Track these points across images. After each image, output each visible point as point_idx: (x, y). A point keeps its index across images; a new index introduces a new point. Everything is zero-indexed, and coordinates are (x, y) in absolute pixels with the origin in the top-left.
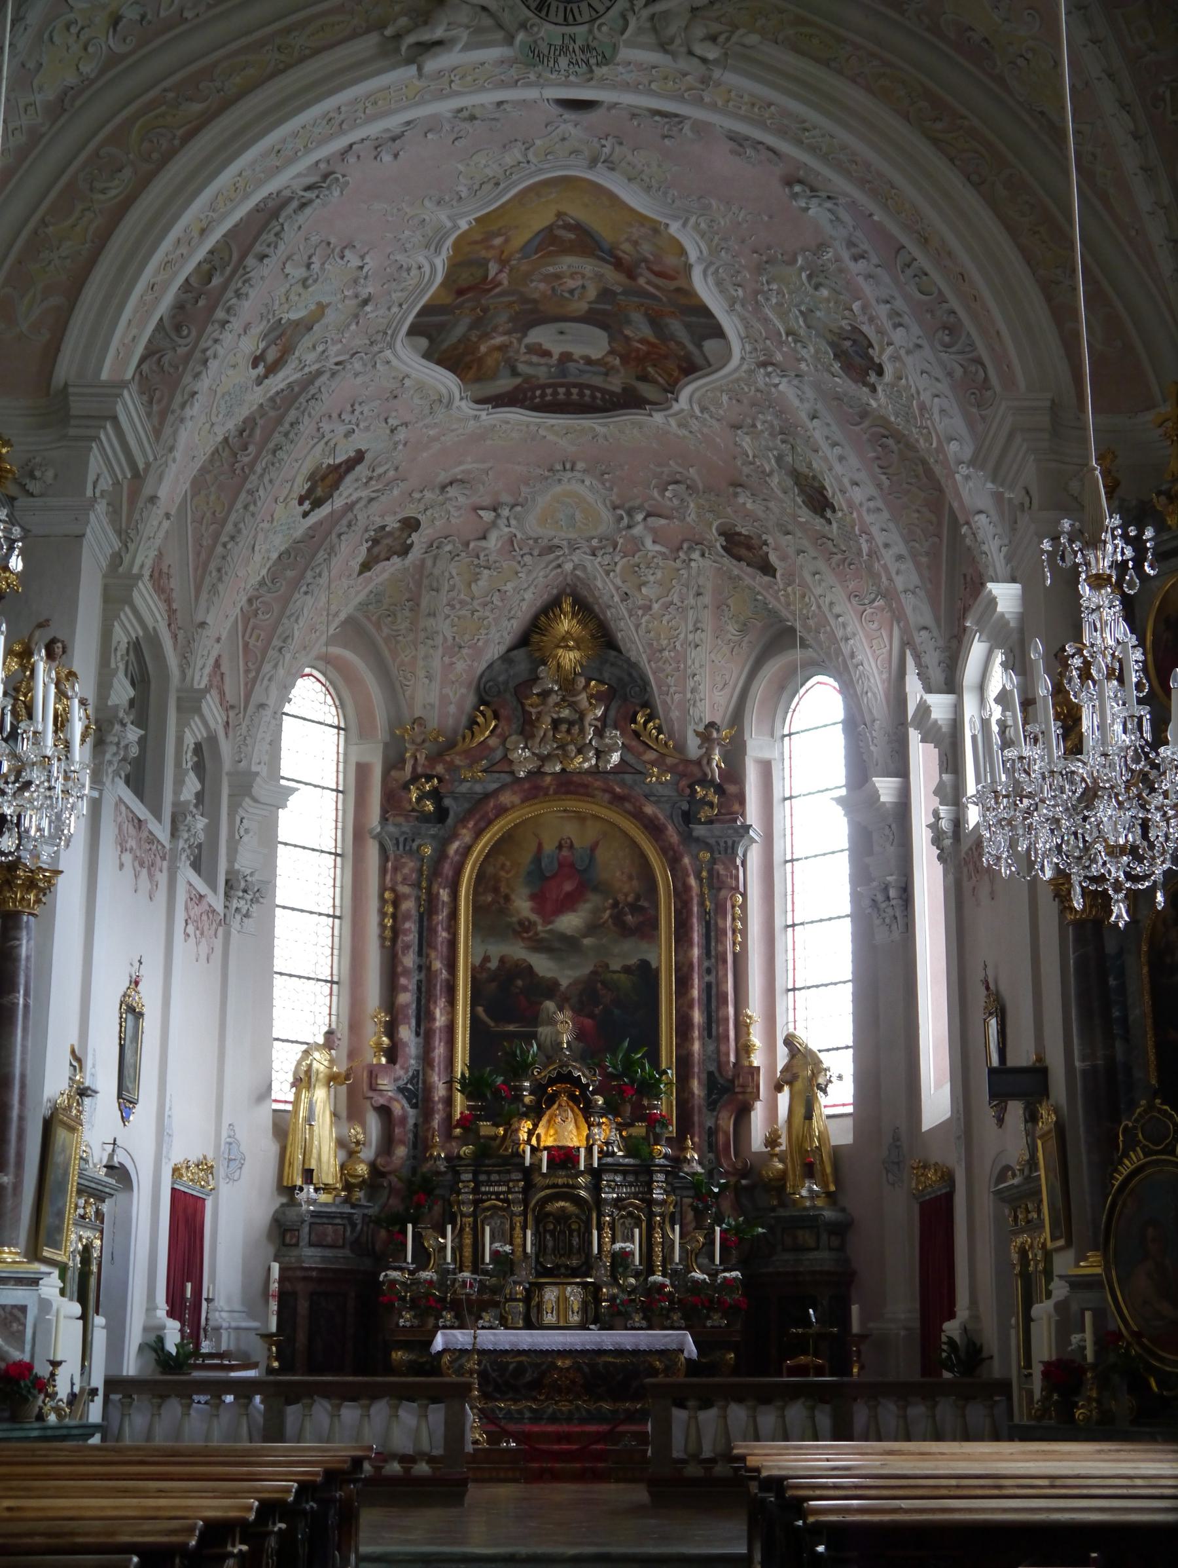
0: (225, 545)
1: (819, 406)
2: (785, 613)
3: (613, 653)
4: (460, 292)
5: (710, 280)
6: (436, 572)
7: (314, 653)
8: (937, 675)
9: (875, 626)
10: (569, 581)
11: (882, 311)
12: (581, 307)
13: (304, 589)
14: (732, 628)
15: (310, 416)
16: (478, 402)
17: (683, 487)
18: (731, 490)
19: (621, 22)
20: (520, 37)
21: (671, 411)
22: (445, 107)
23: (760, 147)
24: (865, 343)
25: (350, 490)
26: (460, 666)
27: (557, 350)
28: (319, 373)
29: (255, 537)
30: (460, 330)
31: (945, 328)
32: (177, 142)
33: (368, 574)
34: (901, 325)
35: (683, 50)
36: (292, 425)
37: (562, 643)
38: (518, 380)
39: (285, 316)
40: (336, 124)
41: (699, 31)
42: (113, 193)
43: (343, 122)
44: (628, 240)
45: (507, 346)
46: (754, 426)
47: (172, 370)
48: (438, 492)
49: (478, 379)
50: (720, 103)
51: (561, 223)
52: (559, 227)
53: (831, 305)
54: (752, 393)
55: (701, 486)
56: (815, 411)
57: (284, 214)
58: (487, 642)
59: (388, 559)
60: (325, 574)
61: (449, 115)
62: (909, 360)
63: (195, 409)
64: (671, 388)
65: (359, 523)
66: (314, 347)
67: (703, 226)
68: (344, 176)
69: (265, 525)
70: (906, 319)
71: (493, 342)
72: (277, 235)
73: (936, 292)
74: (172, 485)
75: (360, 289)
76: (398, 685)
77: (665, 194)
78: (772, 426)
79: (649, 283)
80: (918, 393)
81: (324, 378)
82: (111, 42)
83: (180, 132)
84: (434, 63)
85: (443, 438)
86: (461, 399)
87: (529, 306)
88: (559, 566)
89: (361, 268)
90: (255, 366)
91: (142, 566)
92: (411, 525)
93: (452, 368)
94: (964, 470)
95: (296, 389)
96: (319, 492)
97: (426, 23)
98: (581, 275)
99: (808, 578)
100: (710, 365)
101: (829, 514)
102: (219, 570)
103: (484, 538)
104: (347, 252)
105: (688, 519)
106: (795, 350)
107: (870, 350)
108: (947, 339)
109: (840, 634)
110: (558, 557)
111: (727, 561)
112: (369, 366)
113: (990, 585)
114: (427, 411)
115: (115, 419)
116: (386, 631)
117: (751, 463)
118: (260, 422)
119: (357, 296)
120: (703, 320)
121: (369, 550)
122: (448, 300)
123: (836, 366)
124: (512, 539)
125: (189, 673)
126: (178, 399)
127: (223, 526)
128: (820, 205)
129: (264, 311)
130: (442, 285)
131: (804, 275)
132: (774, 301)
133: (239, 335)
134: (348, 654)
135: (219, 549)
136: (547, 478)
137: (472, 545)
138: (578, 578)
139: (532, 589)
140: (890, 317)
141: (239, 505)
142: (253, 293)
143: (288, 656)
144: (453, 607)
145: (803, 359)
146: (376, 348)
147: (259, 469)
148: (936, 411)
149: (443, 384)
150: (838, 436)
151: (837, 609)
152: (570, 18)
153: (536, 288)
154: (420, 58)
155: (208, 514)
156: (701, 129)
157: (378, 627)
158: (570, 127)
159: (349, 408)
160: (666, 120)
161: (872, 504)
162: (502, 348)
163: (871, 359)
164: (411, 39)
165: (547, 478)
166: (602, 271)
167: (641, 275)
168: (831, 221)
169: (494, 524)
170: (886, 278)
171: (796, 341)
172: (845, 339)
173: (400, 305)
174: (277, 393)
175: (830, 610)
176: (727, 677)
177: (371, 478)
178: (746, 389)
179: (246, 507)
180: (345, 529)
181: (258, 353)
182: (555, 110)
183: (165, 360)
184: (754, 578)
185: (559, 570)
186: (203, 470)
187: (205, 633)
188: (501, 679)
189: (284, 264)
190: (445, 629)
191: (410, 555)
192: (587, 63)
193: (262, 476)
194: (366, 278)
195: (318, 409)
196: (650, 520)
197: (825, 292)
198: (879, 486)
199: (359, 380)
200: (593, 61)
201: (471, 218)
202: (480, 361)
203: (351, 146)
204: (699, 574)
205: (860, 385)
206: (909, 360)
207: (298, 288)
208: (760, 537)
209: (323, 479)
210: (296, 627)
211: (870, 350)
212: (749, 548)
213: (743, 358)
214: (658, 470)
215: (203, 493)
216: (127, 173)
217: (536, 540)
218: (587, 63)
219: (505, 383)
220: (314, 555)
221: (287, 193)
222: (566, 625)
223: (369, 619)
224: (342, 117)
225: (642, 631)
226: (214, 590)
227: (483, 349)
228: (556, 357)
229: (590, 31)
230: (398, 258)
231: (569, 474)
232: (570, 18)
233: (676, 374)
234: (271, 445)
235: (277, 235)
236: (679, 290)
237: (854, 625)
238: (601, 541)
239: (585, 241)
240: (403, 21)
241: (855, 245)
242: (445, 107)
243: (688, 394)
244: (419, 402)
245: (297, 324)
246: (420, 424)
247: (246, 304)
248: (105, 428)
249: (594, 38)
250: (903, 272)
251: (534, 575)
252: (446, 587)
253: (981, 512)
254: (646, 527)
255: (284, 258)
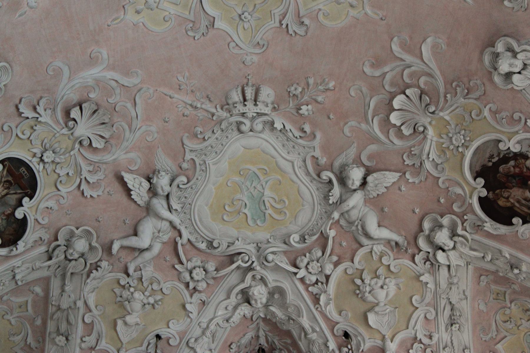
6: (64, 306)
103: (136, 234)
105: (428, 165)
191: (21, 244)
214: (377, 73)
231: (251, 109)
254: (367, 201)
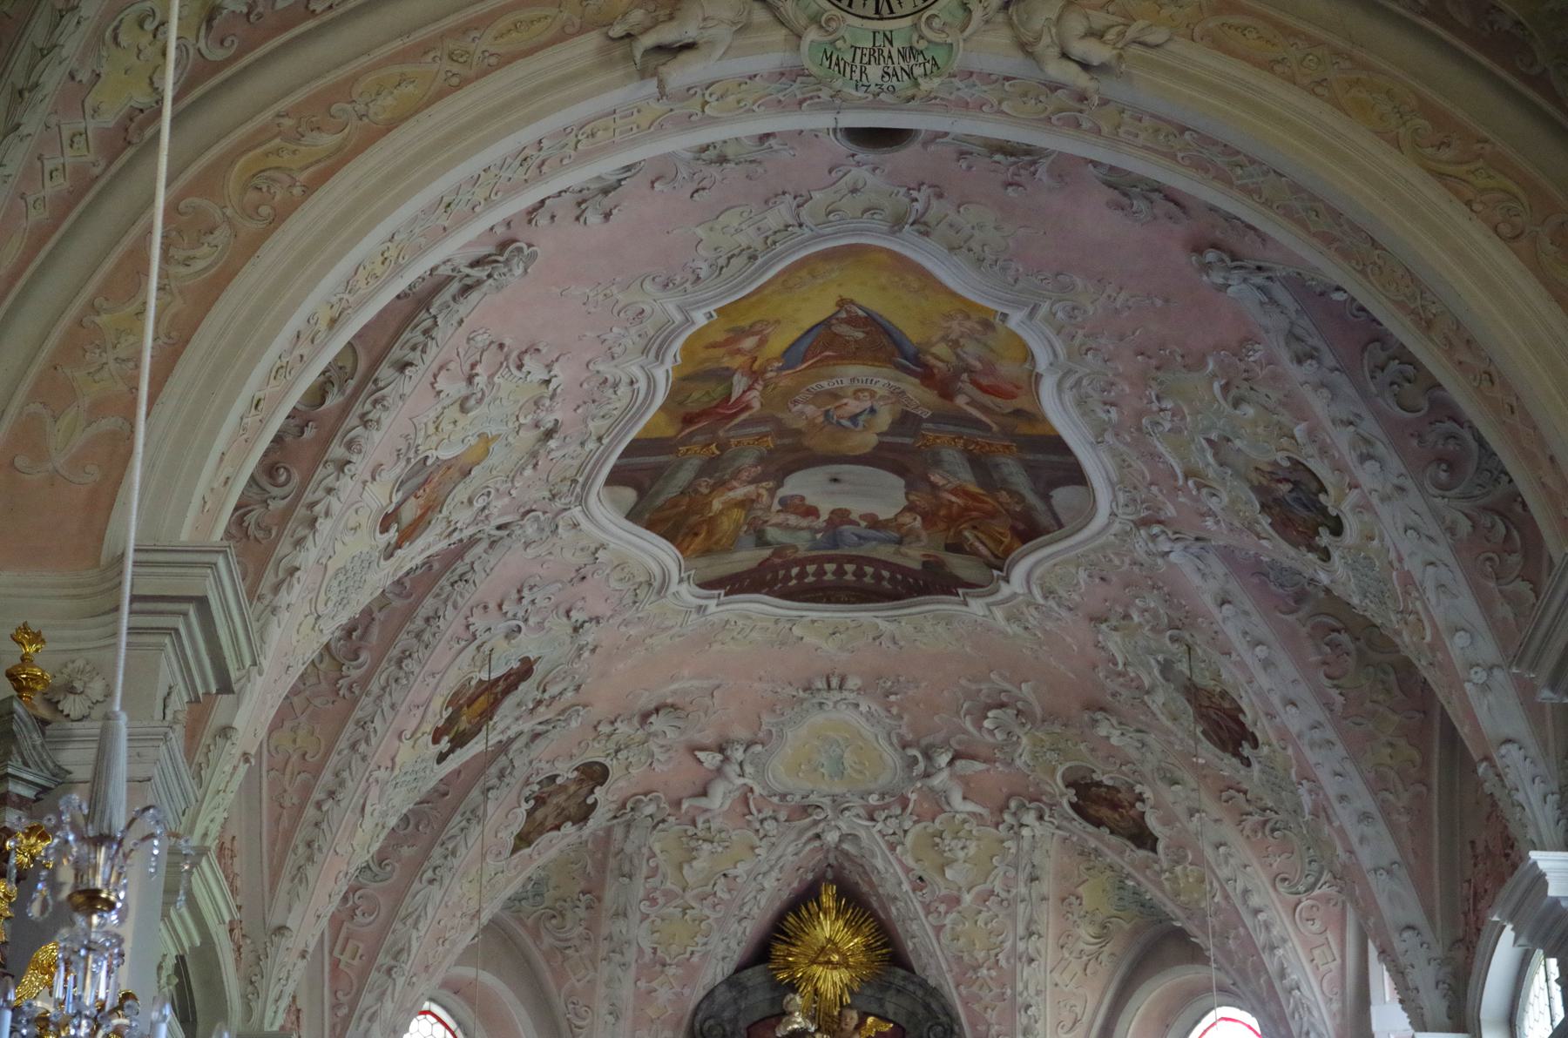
0: (319, 805)
1: (1234, 586)
2: (1170, 907)
3: (901, 972)
4: (688, 420)
5: (1068, 397)
6: (629, 848)
7: (438, 978)
8: (1433, 1002)
9: (1317, 927)
10: (832, 860)
11: (1342, 440)
12: (867, 440)
13: (429, 874)
14: (1086, 932)
15: (455, 607)
16: (705, 585)
17: (1011, 712)
18: (1086, 717)
19: (960, 13)
20: (812, 35)
21: (999, 597)
22: (680, 143)
23: (1156, 196)
24: (1314, 486)
25: (509, 721)
26: (664, 994)
27: (825, 508)
28: (473, 541)
29: (367, 791)
30: (684, 477)
31: (1440, 460)
32: (297, 191)
33: (527, 851)
34: (1370, 457)
35: (1055, 51)
36: (427, 620)
37: (821, 956)
38: (767, 553)
39: (433, 454)
40: (533, 163)
41: (1076, 25)
42: (199, 265)
43: (543, 163)
44: (944, 339)
45: (753, 501)
46: (1127, 616)
47: (260, 534)
48: (636, 721)
49: (706, 552)
50: (1105, 130)
51: (843, 315)
52: (842, 321)
53: (1260, 430)
54: (1126, 567)
55: (1038, 712)
56: (1227, 592)
57: (437, 302)
58: (705, 955)
59: (558, 828)
60: (462, 851)
61: (689, 155)
62: (1384, 511)
63: (295, 595)
64: (999, 563)
65: (515, 773)
66: (470, 501)
67: (1060, 315)
68: (530, 246)
69: (382, 774)
70: (1380, 449)
71: (731, 494)
72: (426, 332)
73: (1425, 405)
74: (252, 714)
75: (543, 414)
76: (564, 1025)
77: (1003, 269)
78: (1156, 616)
79: (972, 403)
80: (1400, 560)
81: (479, 549)
82: (202, 44)
83: (302, 177)
84: (682, 73)
85: (648, 641)
86: (681, 581)
87: (787, 441)
88: (818, 836)
89: (548, 382)
90: (385, 529)
91: (205, 835)
92: (595, 774)
93: (669, 536)
94: (1480, 676)
95: (436, 566)
96: (463, 724)
97: (671, 17)
98: (871, 392)
99: (1209, 852)
100: (1061, 526)
101: (1246, 750)
102: (309, 845)
103: (704, 793)
104: (527, 359)
105: (1018, 763)
106: (1197, 500)
107: (1322, 497)
108: (1443, 476)
109: (1260, 939)
110: (816, 823)
111: (1079, 824)
112: (547, 532)
113: (1534, 855)
114: (628, 600)
115: (202, 602)
116: (548, 941)
117: (1120, 674)
118: (379, 616)
119: (537, 426)
120: (1054, 458)
121: (530, 813)
122: (670, 432)
123: (1265, 521)
124: (746, 796)
125: (257, 1007)
126: (269, 578)
127: (316, 777)
128: (1245, 280)
129: (404, 448)
130: (662, 408)
131: (1216, 386)
132: (1168, 426)
133: (365, 483)
134: (487, 978)
135: (310, 812)
136: (802, 701)
137: (685, 806)
138: (846, 854)
139: (775, 874)
140: (1353, 447)
141: (343, 743)
142: (386, 420)
143: (401, 981)
144: (653, 901)
145: (1211, 513)
146: (558, 504)
147: (374, 687)
148: (1429, 585)
149: (655, 558)
150: (1262, 630)
151: (1255, 901)
152: (885, 10)
153: (802, 413)
154: (662, 69)
155: (295, 758)
156: (1066, 170)
157: (537, 936)
158: (862, 174)
159: (515, 596)
160: (1013, 159)
161: (1317, 734)
162: (746, 504)
163: (1323, 510)
164: (649, 40)
165: (802, 701)
166: (903, 386)
167: (960, 391)
168: (1262, 303)
169: (719, 772)
170: (1348, 389)
171: (1199, 486)
172: (1279, 481)
173: (600, 439)
174: (408, 573)
175: (1245, 902)
176: (1078, 1010)
177: (539, 703)
178: (1117, 562)
179: (353, 747)
180: (495, 781)
181: (390, 509)
182: (843, 147)
183: (251, 519)
184: (1121, 853)
185: (817, 843)
186: (295, 691)
187: (285, 942)
188: (727, 1015)
189: (435, 376)
190: (641, 935)
191: (591, 822)
192: (910, 74)
193: (380, 698)
194: (552, 398)
195: (469, 596)
196: (959, 763)
197: (1249, 411)
198: (1328, 706)
199: (531, 552)
200: (918, 71)
201: (711, 309)
202: (712, 522)
203: (543, 202)
204: (1033, 848)
205: (1304, 549)
206: (1384, 511)
207: (454, 412)
208: (1131, 788)
209: (471, 702)
210: (415, 934)
211: (1322, 497)
212: (1115, 806)
213: (1113, 514)
214: (974, 687)
215: (288, 724)
216: (221, 235)
217: (783, 797)
218: (910, 74)
219: (746, 558)
220: (448, 820)
221: (445, 271)
222: (827, 928)
223: (524, 925)
224: (543, 154)
225: (945, 937)
226: (300, 875)
227: (717, 505)
228: (824, 516)
229: (915, 26)
230: (601, 368)
231: (836, 695)
232: (885, 10)
233: (1007, 540)
234: (395, 652)
235: (426, 332)
236: (1018, 413)
237: (1282, 924)
238: (882, 796)
239: (878, 341)
240: (638, 16)
241: (1299, 339)
242: (680, 143)
243: (1027, 569)
244: (614, 584)
245: (448, 465)
246: (618, 619)
247: (377, 436)
248: (185, 614)
249: (921, 37)
250: (1373, 377)
251: (778, 853)
252: (645, 871)
253: (1509, 741)
255: (435, 367)
